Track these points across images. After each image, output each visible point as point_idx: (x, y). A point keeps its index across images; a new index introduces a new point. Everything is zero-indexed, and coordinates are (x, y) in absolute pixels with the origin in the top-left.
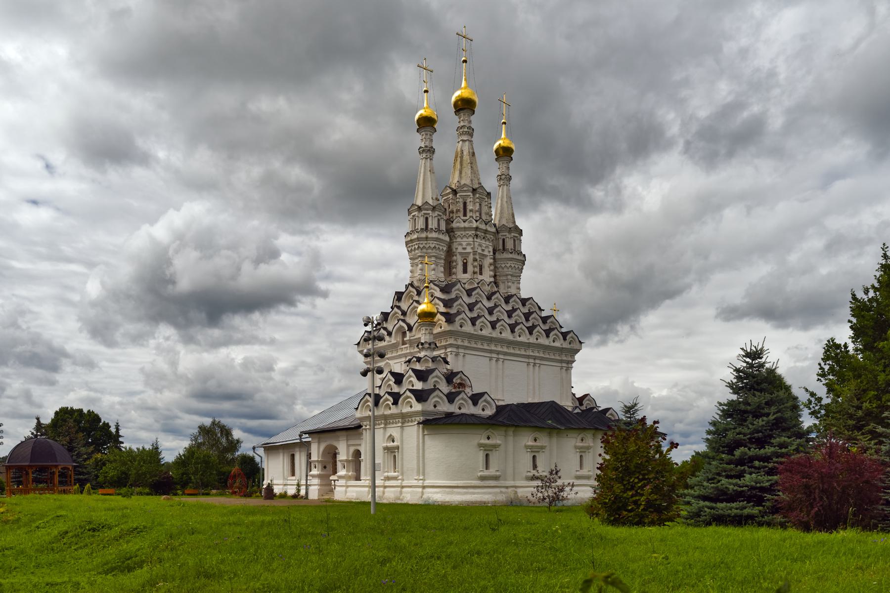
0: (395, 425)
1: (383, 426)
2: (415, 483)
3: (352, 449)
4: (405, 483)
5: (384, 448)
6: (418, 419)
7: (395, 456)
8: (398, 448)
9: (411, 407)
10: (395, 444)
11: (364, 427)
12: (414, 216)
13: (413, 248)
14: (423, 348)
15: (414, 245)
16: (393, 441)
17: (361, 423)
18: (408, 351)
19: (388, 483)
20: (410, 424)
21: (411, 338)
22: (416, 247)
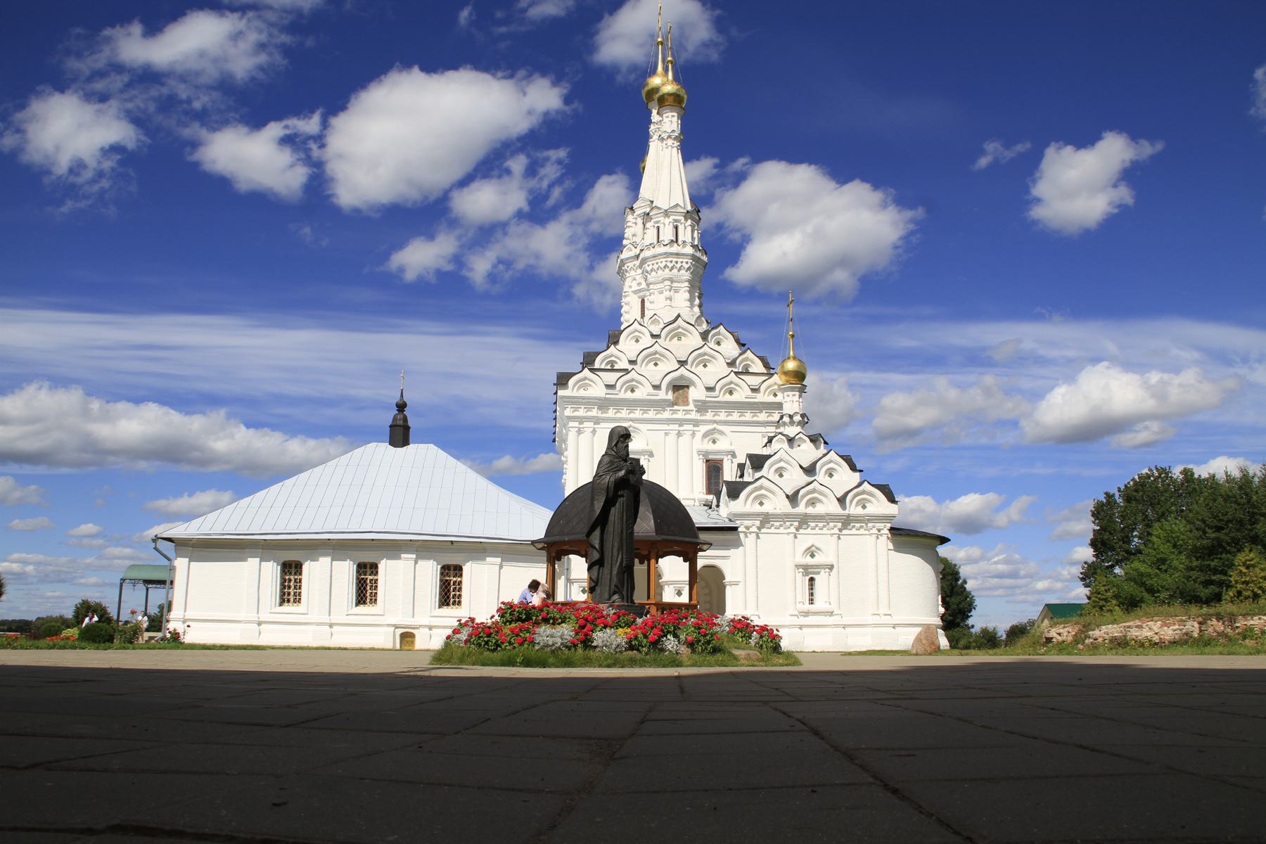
0: (817, 531)
1: (793, 530)
2: (876, 620)
5: (796, 566)
6: (880, 525)
8: (831, 567)
9: (864, 507)
10: (818, 559)
12: (676, 221)
13: (678, 265)
15: (682, 262)
16: (812, 556)
18: (688, 417)
19: (803, 621)
20: (854, 531)
22: (687, 266)
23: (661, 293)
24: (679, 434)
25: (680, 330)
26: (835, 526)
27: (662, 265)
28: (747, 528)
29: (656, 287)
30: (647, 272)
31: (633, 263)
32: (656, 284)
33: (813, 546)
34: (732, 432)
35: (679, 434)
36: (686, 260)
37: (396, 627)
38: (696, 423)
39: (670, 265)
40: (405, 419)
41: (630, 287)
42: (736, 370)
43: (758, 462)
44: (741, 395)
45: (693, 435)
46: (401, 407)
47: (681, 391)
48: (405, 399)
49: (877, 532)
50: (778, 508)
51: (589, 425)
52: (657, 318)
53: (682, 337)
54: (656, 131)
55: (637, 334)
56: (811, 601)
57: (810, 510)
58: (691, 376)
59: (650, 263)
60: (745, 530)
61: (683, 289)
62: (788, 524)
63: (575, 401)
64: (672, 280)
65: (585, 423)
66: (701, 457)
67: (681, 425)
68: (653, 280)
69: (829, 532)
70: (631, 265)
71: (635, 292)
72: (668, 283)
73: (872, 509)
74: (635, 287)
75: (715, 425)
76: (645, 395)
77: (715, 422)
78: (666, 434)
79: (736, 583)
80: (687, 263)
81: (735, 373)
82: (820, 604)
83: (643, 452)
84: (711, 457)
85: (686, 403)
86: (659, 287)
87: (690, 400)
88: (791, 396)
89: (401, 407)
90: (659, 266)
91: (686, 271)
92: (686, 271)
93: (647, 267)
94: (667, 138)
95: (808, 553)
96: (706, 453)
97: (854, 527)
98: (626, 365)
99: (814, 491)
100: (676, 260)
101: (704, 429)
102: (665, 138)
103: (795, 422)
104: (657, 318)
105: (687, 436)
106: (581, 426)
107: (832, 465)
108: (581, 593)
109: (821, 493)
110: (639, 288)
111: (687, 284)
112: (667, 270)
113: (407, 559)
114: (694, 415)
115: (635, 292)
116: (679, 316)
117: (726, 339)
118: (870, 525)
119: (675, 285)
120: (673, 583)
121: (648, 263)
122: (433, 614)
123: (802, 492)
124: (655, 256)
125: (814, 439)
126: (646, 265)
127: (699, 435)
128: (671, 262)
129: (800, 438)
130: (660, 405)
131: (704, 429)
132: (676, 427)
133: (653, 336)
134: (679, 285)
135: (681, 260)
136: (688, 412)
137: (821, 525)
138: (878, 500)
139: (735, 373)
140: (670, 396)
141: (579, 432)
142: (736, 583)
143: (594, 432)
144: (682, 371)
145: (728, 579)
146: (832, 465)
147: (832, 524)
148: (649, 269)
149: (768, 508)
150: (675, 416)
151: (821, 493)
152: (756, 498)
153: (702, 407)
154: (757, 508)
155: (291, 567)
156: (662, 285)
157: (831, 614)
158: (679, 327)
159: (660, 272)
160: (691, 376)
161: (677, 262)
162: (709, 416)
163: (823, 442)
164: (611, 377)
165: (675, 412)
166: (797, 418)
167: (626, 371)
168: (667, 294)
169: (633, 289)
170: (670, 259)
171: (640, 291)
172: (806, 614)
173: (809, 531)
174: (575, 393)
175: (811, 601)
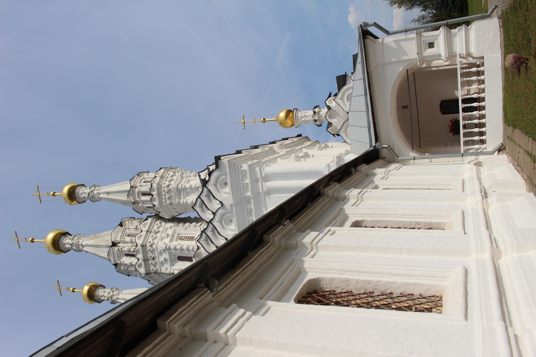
29: (183, 183)
30: (168, 186)
31: (151, 235)
41: (165, 243)
54: (78, 240)
59: (164, 182)
70: (150, 239)
71: (171, 241)
74: (167, 241)
90: (171, 177)
93: (165, 185)
94: (94, 188)
102: (93, 189)
110: (169, 238)
112: (177, 174)
115: (171, 241)
124: (162, 177)
126: (163, 185)
148: (167, 183)
156: (184, 180)
159: (175, 178)
171: (173, 236)
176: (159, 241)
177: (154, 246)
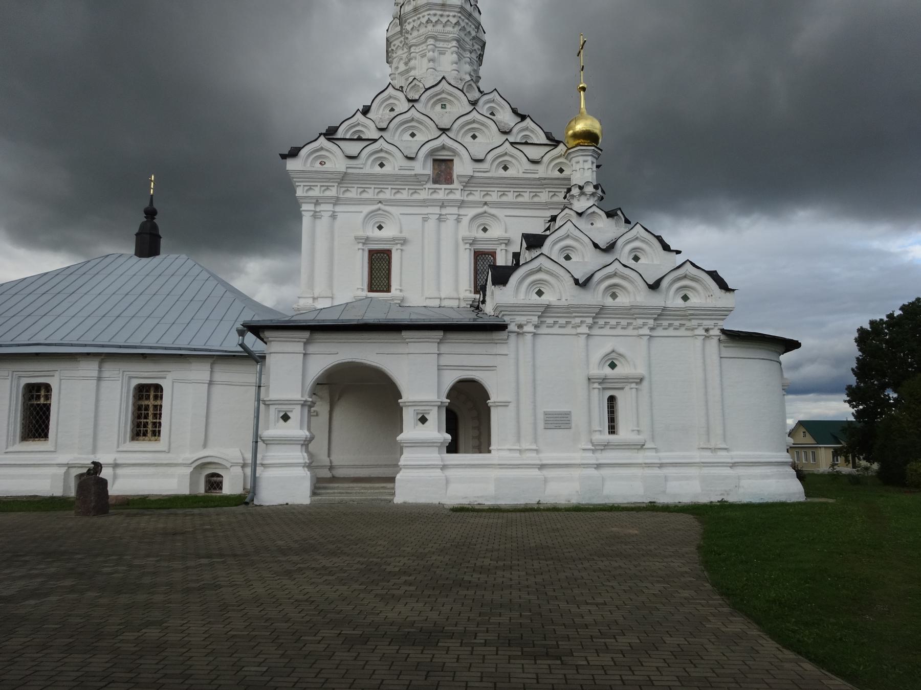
0: (619, 331)
1: (584, 329)
2: (708, 456)
3: (451, 378)
4: (666, 456)
5: (589, 379)
6: (708, 323)
7: (612, 399)
8: (641, 380)
10: (620, 371)
11: (512, 327)
13: (444, 20)
14: (582, 193)
15: (448, 16)
16: (613, 366)
17: (507, 319)
18: (451, 197)
21: (477, 174)
22: (454, 21)
23: (423, 56)
24: (441, 219)
25: (443, 96)
26: (644, 324)
27: (424, 20)
28: (520, 326)
30: (407, 32)
32: (419, 45)
33: (613, 351)
34: (506, 216)
35: (441, 219)
36: (452, 14)
37: (70, 466)
38: (462, 204)
39: (434, 19)
40: (155, 227)
42: (512, 139)
43: (534, 242)
44: (519, 169)
45: (458, 221)
46: (151, 213)
47: (443, 167)
48: (156, 206)
49: (703, 333)
50: (564, 300)
51: (326, 207)
52: (418, 83)
53: (448, 106)
55: (391, 101)
56: (612, 430)
57: (609, 301)
58: (455, 145)
60: (516, 329)
61: (450, 51)
62: (578, 320)
63: (312, 177)
64: (435, 38)
65: (322, 205)
66: (468, 246)
67: (442, 206)
68: (414, 41)
69: (635, 332)
72: (431, 41)
73: (695, 301)
75: (486, 208)
76: (397, 169)
77: (486, 203)
78: (425, 220)
79: (505, 404)
80: (454, 16)
81: (512, 144)
82: (625, 433)
83: (394, 240)
84: (480, 247)
85: (449, 181)
86: (421, 49)
87: (455, 177)
88: (581, 162)
89: (151, 213)
91: (453, 27)
92: (453, 27)
95: (606, 362)
96: (474, 241)
97: (670, 325)
98: (375, 135)
99: (615, 275)
100: (440, 13)
101: (472, 212)
103: (586, 195)
104: (418, 83)
105: (450, 223)
106: (318, 209)
107: (637, 244)
108: (281, 421)
109: (624, 277)
111: (454, 43)
112: (430, 27)
113: (85, 378)
114: (457, 196)
116: (444, 78)
117: (502, 108)
118: (694, 323)
119: (441, 44)
120: (415, 404)
121: (408, 21)
122: (120, 449)
123: (597, 277)
125: (610, 215)
127: (465, 221)
128: (435, 15)
129: (594, 212)
130: (417, 181)
131: (472, 212)
132: (437, 210)
133: (409, 101)
134: (445, 45)
135: (447, 13)
136: (451, 191)
137: (624, 322)
138: (706, 288)
139: (512, 144)
140: (429, 170)
141: (316, 216)
142: (505, 404)
143: (334, 216)
144: (444, 139)
145: (494, 398)
146: (637, 244)
147: (640, 322)
149: (548, 298)
150: (435, 196)
151: (624, 277)
152: (534, 283)
153: (469, 182)
154: (535, 298)
155: (148, 391)
156: (424, 46)
157: (641, 447)
158: (443, 92)
160: (455, 145)
161: (442, 16)
162: (477, 196)
163: (623, 219)
164: (353, 148)
165: (435, 191)
166: (590, 189)
167: (375, 141)
168: (431, 53)
169: (399, 71)
170: (432, 12)
172: (606, 446)
173: (606, 331)
174: (308, 167)
175: (612, 430)
176: (397, 58)
177: (394, 55)
